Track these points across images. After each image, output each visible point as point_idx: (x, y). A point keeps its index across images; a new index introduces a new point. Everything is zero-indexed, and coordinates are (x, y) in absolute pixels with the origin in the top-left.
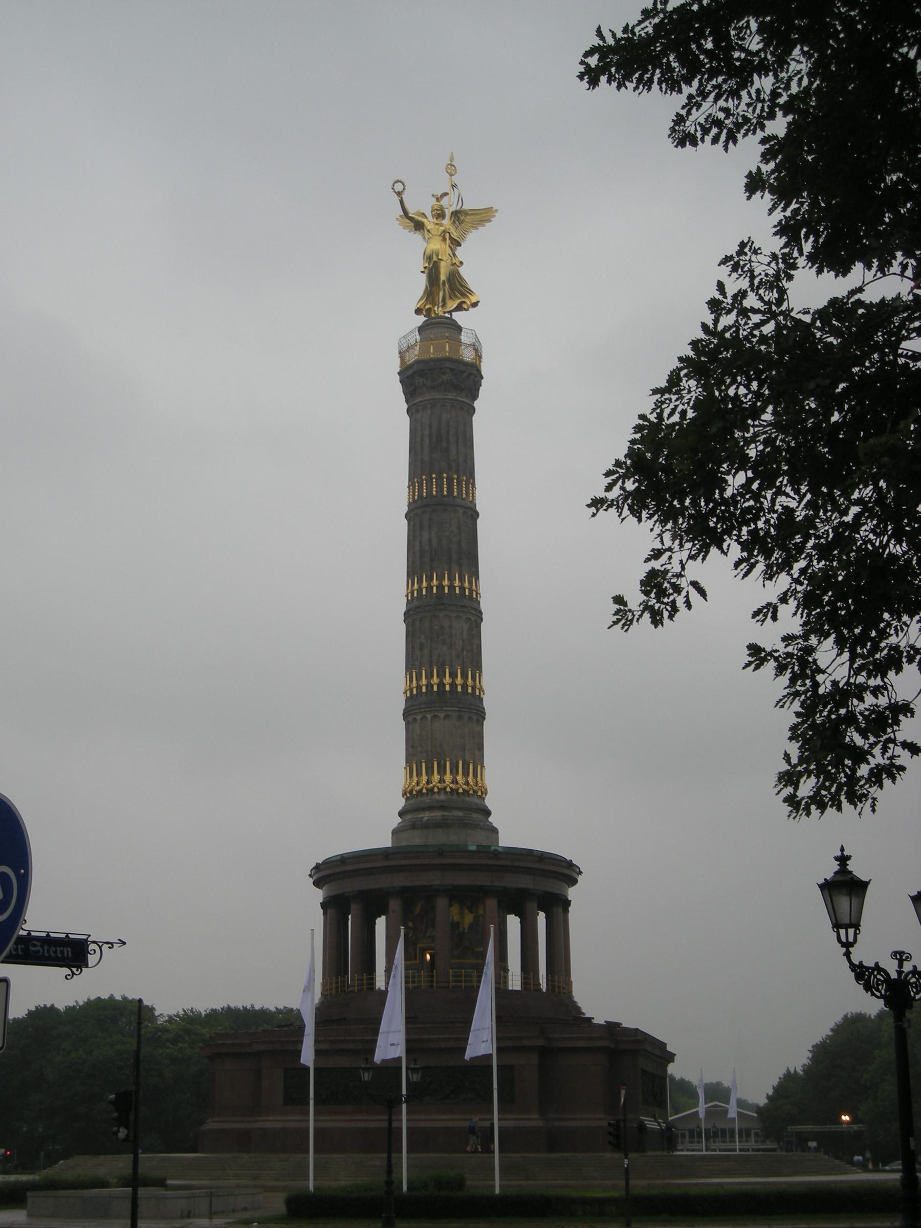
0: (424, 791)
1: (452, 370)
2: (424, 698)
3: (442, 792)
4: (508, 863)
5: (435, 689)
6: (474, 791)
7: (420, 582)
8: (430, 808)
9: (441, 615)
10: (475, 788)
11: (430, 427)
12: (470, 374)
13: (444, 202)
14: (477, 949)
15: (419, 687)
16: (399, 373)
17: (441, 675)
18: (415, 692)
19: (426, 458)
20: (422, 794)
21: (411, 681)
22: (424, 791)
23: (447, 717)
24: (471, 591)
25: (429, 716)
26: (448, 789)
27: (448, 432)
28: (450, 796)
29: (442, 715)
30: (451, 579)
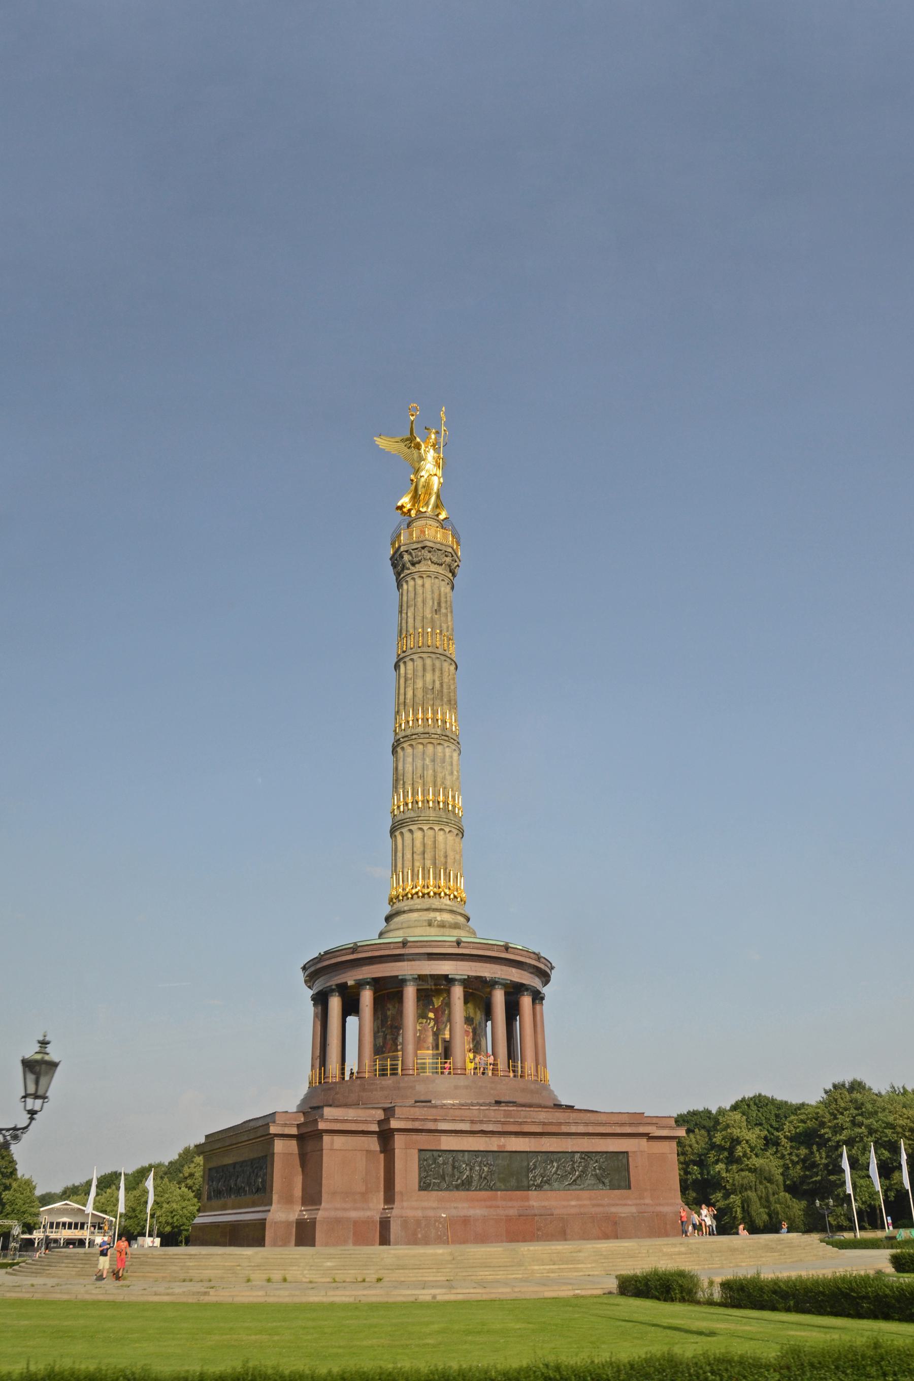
9: (446, 744)
11: (433, 592)
19: (429, 616)
22: (432, 894)
26: (452, 896)
27: (446, 602)
29: (447, 830)
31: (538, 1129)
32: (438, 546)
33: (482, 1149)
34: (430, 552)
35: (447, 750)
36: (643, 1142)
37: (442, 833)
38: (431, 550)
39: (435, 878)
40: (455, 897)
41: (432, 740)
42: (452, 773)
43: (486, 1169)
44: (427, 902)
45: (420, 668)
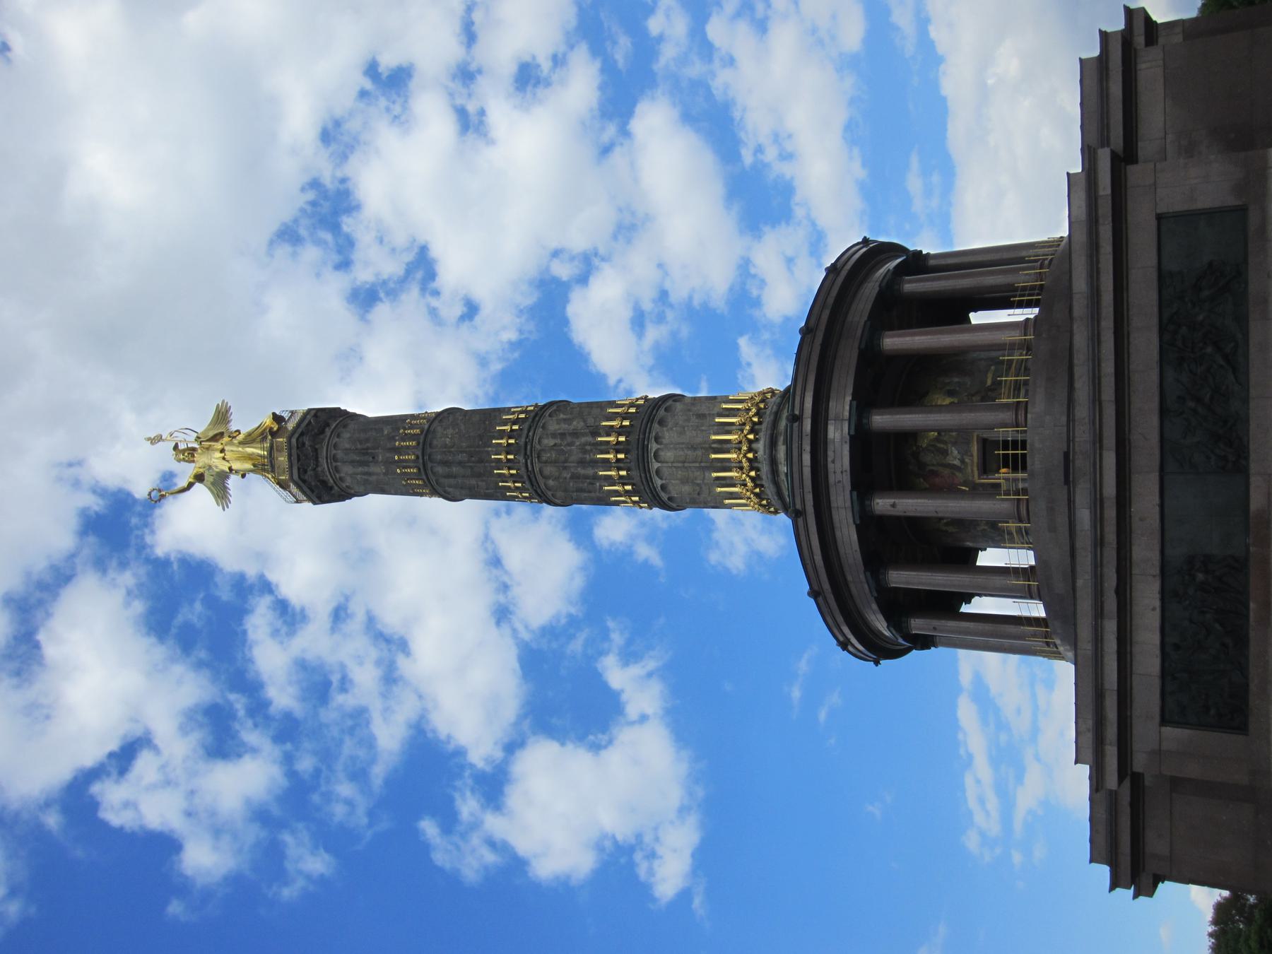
0: (753, 474)
1: (302, 434)
2: (635, 473)
3: (754, 446)
4: (826, 313)
5: (621, 456)
6: (762, 401)
7: (503, 478)
8: (773, 462)
10: (757, 399)
12: (315, 416)
13: (182, 446)
14: (989, 382)
15: (623, 481)
16: (315, 503)
17: (605, 448)
18: (628, 488)
20: (758, 477)
21: (617, 493)
22: (753, 474)
23: (657, 439)
24: (521, 412)
25: (656, 465)
26: (751, 437)
28: (762, 434)
30: (502, 434)
31: (1110, 459)
32: (294, 458)
33: (1156, 586)
34: (305, 472)
35: (545, 441)
36: (1135, 174)
37: (661, 453)
38: (302, 471)
39: (730, 470)
40: (751, 431)
41: (537, 469)
42: (575, 434)
43: (1200, 576)
44: (766, 481)
45: (452, 481)
